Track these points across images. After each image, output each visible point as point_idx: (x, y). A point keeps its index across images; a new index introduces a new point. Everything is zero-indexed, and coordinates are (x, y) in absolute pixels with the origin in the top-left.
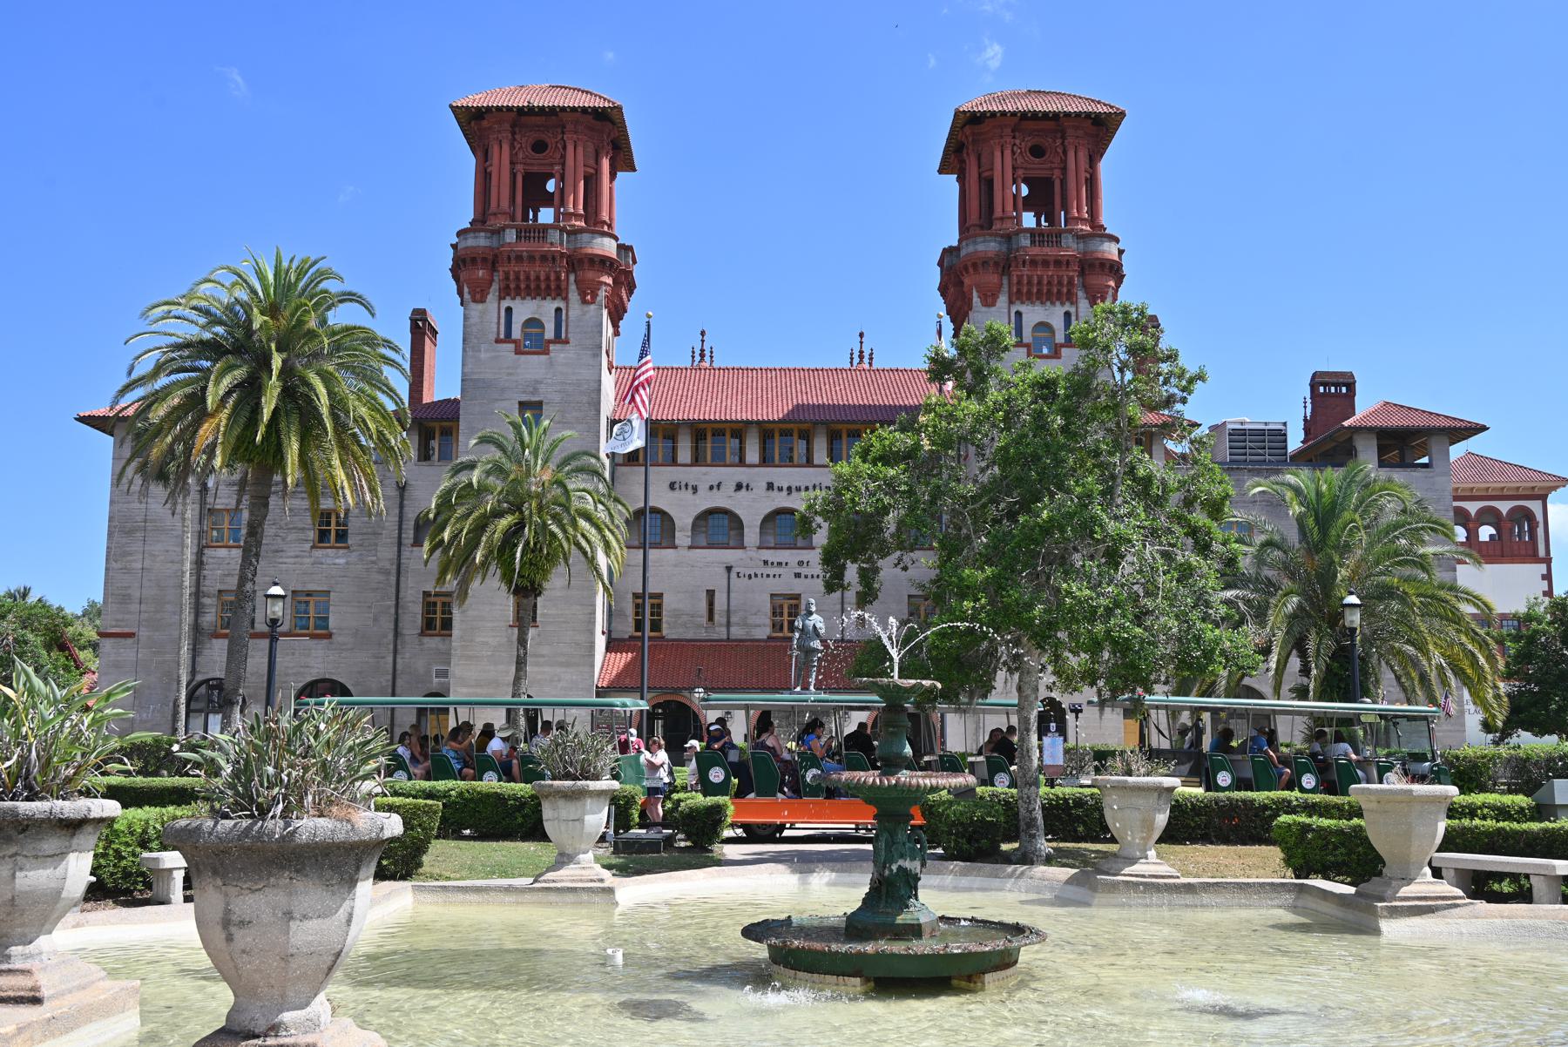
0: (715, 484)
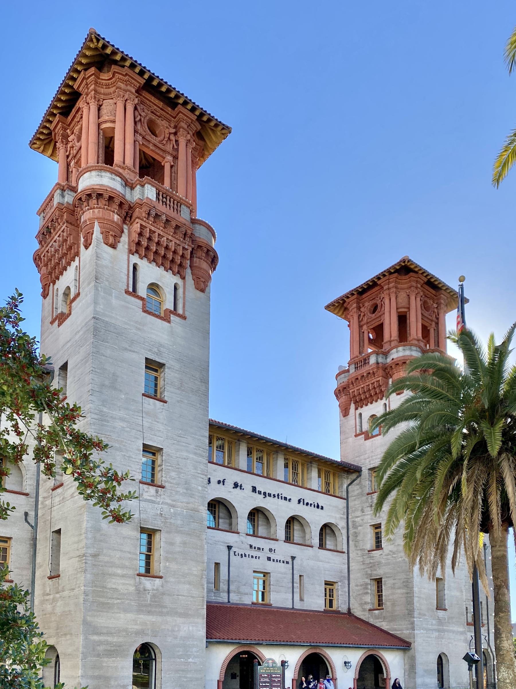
0: (222, 480)
